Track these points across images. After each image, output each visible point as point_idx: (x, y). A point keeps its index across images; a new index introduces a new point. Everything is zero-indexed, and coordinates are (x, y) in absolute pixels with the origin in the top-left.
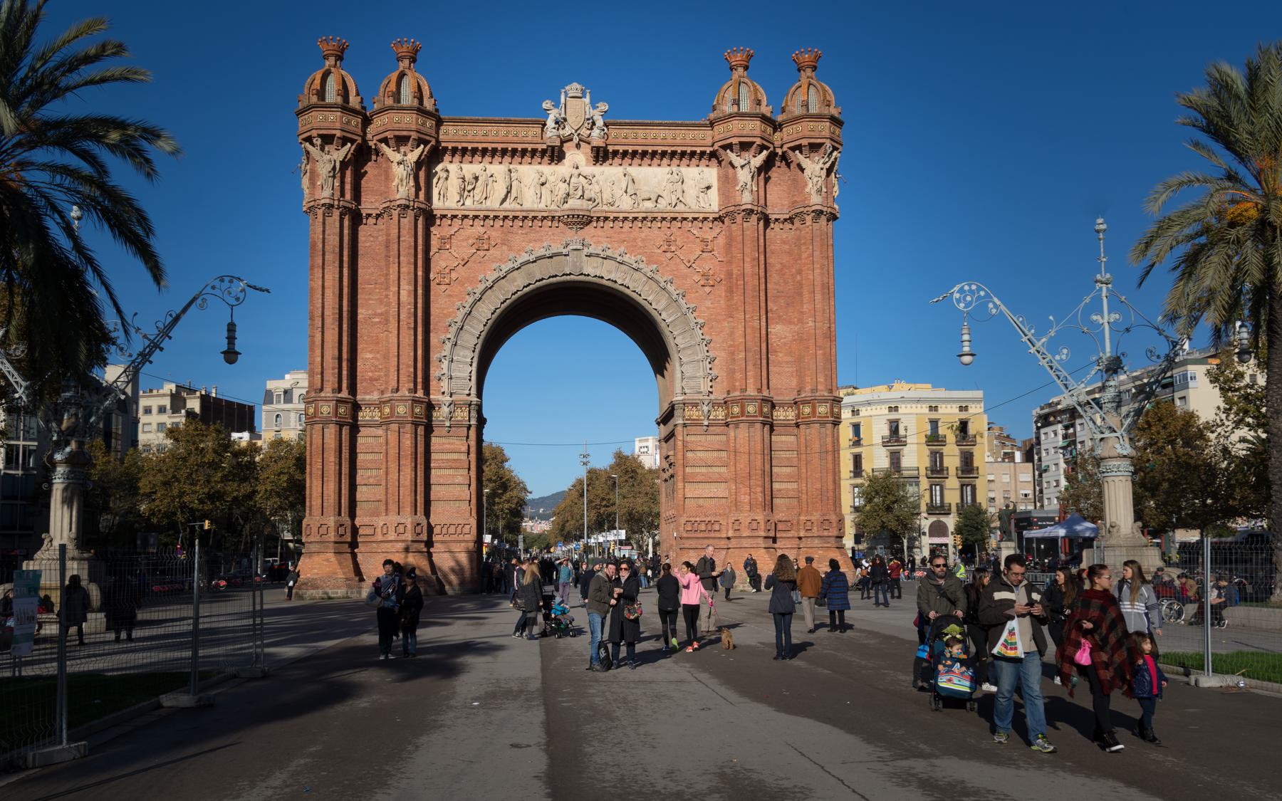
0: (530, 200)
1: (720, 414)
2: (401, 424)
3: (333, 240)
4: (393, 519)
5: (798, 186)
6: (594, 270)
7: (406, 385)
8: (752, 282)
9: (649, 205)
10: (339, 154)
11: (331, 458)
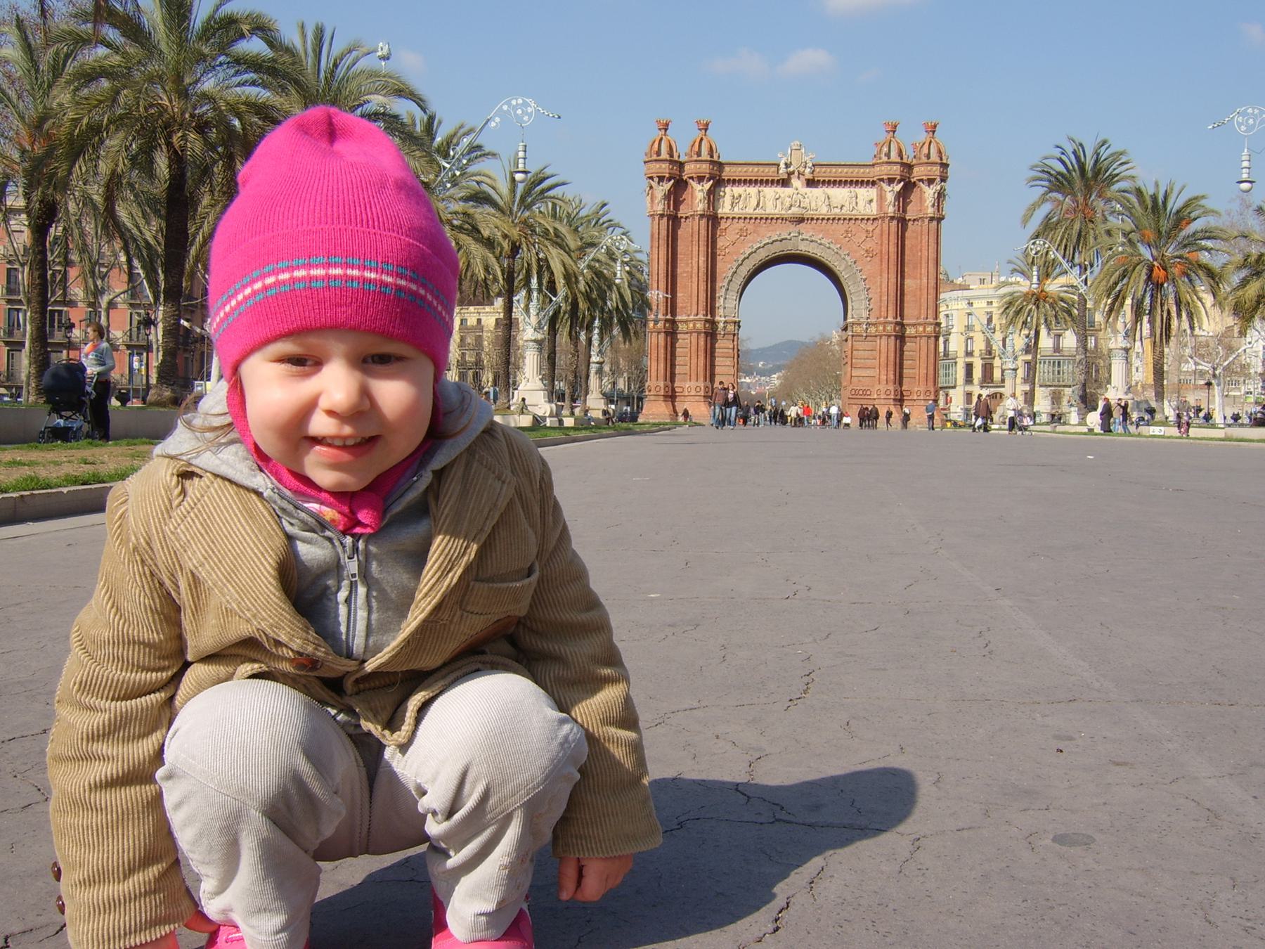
0: (770, 209)
1: (872, 330)
2: (699, 333)
3: (664, 233)
4: (693, 384)
5: (922, 200)
6: (804, 248)
7: (702, 312)
8: (893, 257)
9: (837, 211)
10: (667, 186)
11: (662, 351)
